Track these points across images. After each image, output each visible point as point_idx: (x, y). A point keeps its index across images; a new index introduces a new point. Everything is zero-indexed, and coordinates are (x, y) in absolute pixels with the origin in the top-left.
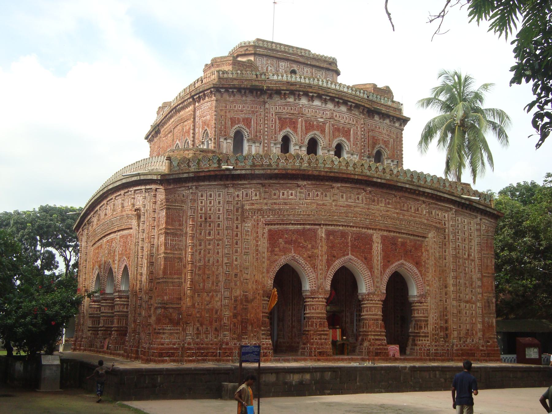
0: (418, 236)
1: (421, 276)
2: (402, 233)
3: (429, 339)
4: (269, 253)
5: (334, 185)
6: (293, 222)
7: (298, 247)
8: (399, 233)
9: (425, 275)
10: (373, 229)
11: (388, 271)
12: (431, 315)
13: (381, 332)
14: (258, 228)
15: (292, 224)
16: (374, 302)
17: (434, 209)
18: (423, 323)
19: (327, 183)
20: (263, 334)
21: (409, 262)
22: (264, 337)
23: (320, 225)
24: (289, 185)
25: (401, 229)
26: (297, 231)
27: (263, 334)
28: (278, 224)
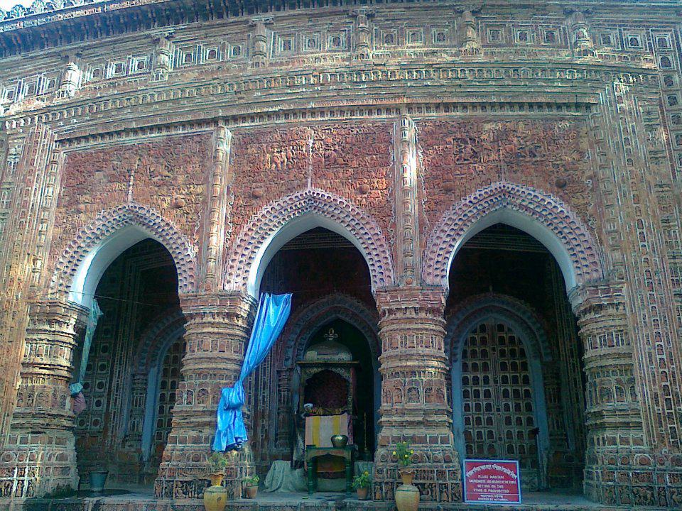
0: (559, 107)
1: (586, 222)
2: (493, 105)
3: (643, 434)
4: (63, 210)
5: (254, 18)
6: (134, 125)
7: (146, 185)
8: (483, 106)
9: (602, 215)
10: (388, 110)
11: (447, 215)
12: (641, 350)
13: (426, 413)
14: (35, 151)
15: (135, 131)
16: (399, 315)
17: (613, 27)
18: (613, 379)
19: (232, 19)
20: (14, 427)
21: (526, 183)
22: (19, 435)
23: (215, 121)
24: (131, 45)
25: (487, 94)
26: (148, 148)
27: (14, 427)
28: (94, 137)
